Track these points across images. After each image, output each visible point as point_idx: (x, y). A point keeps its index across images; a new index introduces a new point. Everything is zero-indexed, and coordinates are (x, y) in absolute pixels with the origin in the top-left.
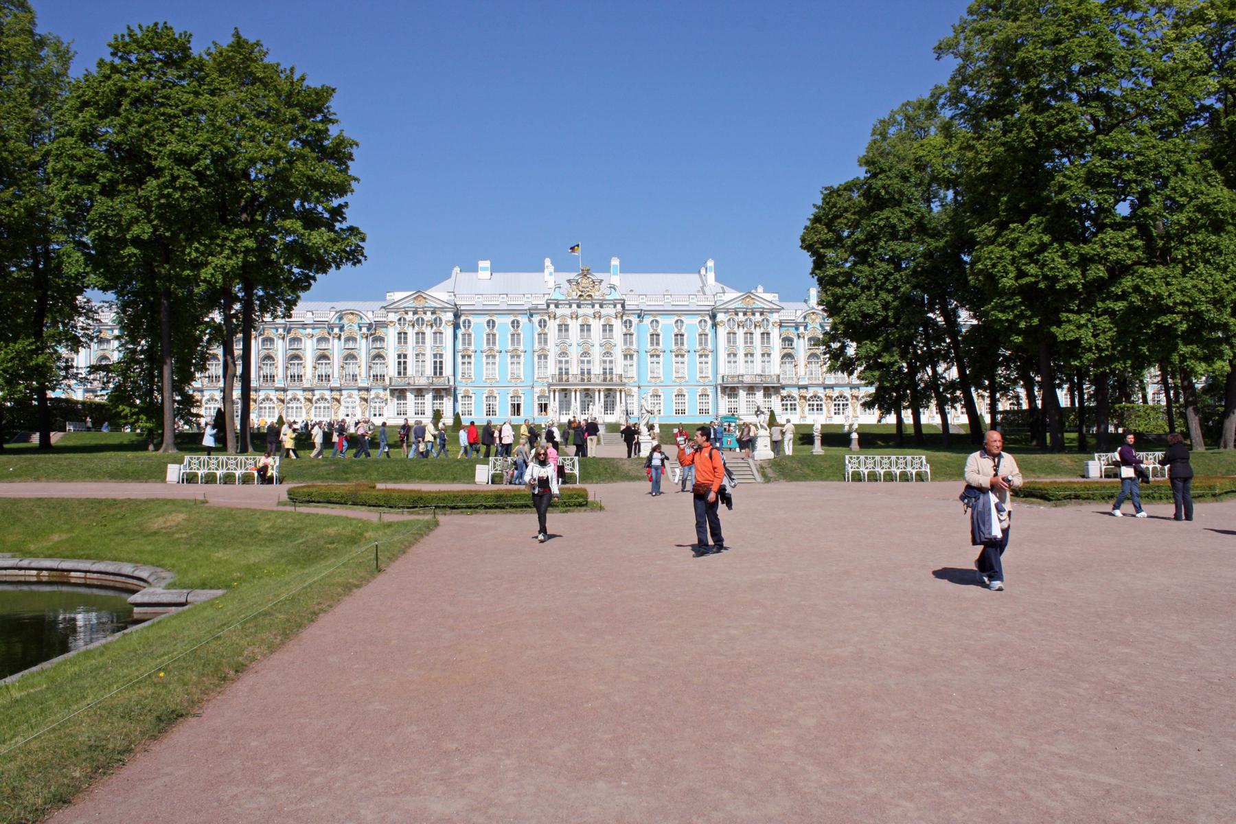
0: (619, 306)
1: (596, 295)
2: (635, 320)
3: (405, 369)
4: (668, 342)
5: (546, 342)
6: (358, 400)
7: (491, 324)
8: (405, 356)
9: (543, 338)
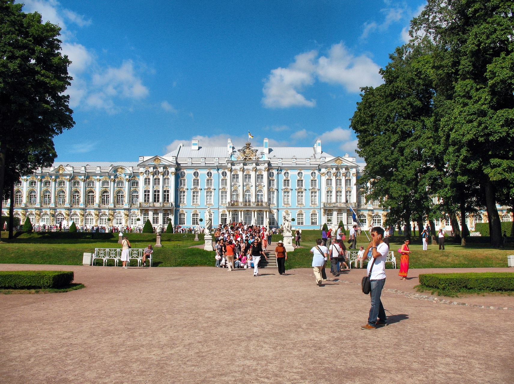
0: (266, 165)
1: (253, 158)
2: (275, 172)
3: (148, 198)
4: (293, 185)
5: (226, 184)
6: (123, 215)
7: (196, 174)
8: (149, 191)
9: (224, 181)
